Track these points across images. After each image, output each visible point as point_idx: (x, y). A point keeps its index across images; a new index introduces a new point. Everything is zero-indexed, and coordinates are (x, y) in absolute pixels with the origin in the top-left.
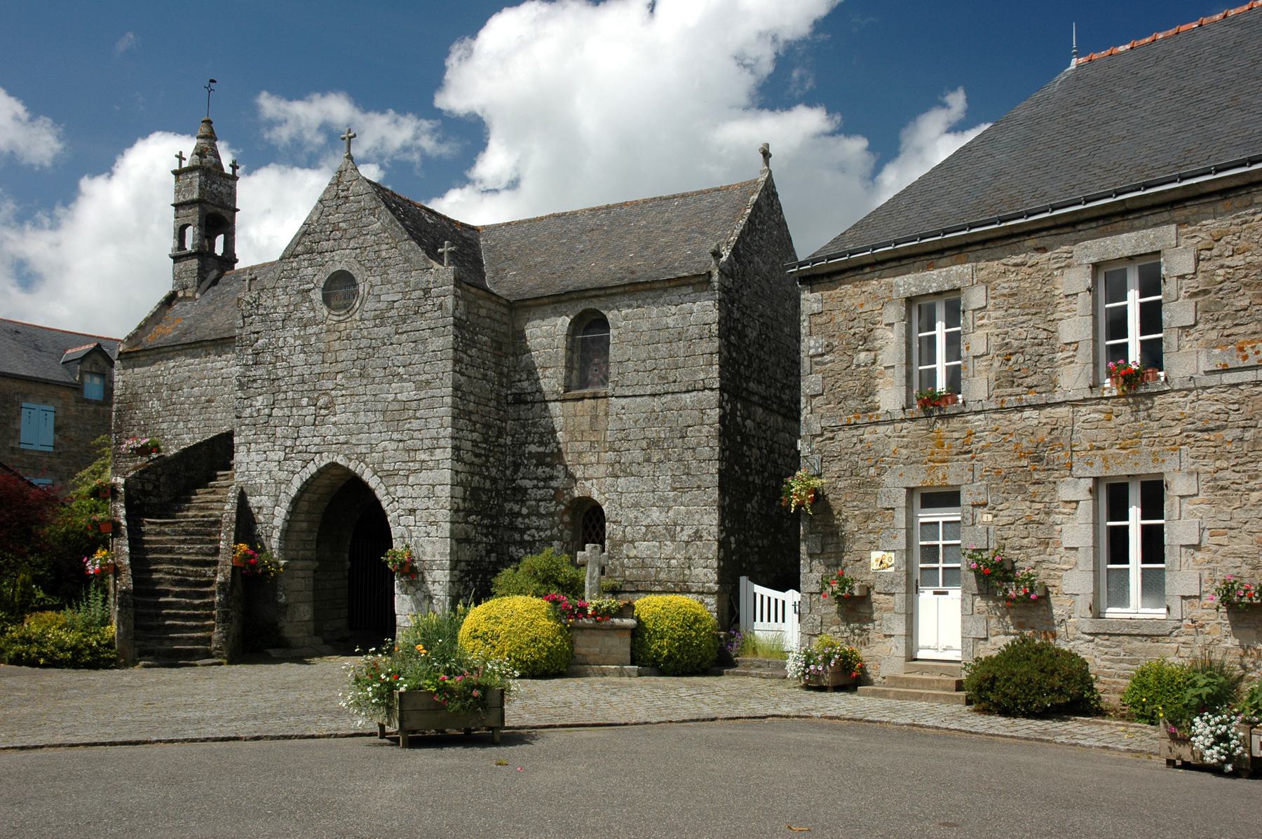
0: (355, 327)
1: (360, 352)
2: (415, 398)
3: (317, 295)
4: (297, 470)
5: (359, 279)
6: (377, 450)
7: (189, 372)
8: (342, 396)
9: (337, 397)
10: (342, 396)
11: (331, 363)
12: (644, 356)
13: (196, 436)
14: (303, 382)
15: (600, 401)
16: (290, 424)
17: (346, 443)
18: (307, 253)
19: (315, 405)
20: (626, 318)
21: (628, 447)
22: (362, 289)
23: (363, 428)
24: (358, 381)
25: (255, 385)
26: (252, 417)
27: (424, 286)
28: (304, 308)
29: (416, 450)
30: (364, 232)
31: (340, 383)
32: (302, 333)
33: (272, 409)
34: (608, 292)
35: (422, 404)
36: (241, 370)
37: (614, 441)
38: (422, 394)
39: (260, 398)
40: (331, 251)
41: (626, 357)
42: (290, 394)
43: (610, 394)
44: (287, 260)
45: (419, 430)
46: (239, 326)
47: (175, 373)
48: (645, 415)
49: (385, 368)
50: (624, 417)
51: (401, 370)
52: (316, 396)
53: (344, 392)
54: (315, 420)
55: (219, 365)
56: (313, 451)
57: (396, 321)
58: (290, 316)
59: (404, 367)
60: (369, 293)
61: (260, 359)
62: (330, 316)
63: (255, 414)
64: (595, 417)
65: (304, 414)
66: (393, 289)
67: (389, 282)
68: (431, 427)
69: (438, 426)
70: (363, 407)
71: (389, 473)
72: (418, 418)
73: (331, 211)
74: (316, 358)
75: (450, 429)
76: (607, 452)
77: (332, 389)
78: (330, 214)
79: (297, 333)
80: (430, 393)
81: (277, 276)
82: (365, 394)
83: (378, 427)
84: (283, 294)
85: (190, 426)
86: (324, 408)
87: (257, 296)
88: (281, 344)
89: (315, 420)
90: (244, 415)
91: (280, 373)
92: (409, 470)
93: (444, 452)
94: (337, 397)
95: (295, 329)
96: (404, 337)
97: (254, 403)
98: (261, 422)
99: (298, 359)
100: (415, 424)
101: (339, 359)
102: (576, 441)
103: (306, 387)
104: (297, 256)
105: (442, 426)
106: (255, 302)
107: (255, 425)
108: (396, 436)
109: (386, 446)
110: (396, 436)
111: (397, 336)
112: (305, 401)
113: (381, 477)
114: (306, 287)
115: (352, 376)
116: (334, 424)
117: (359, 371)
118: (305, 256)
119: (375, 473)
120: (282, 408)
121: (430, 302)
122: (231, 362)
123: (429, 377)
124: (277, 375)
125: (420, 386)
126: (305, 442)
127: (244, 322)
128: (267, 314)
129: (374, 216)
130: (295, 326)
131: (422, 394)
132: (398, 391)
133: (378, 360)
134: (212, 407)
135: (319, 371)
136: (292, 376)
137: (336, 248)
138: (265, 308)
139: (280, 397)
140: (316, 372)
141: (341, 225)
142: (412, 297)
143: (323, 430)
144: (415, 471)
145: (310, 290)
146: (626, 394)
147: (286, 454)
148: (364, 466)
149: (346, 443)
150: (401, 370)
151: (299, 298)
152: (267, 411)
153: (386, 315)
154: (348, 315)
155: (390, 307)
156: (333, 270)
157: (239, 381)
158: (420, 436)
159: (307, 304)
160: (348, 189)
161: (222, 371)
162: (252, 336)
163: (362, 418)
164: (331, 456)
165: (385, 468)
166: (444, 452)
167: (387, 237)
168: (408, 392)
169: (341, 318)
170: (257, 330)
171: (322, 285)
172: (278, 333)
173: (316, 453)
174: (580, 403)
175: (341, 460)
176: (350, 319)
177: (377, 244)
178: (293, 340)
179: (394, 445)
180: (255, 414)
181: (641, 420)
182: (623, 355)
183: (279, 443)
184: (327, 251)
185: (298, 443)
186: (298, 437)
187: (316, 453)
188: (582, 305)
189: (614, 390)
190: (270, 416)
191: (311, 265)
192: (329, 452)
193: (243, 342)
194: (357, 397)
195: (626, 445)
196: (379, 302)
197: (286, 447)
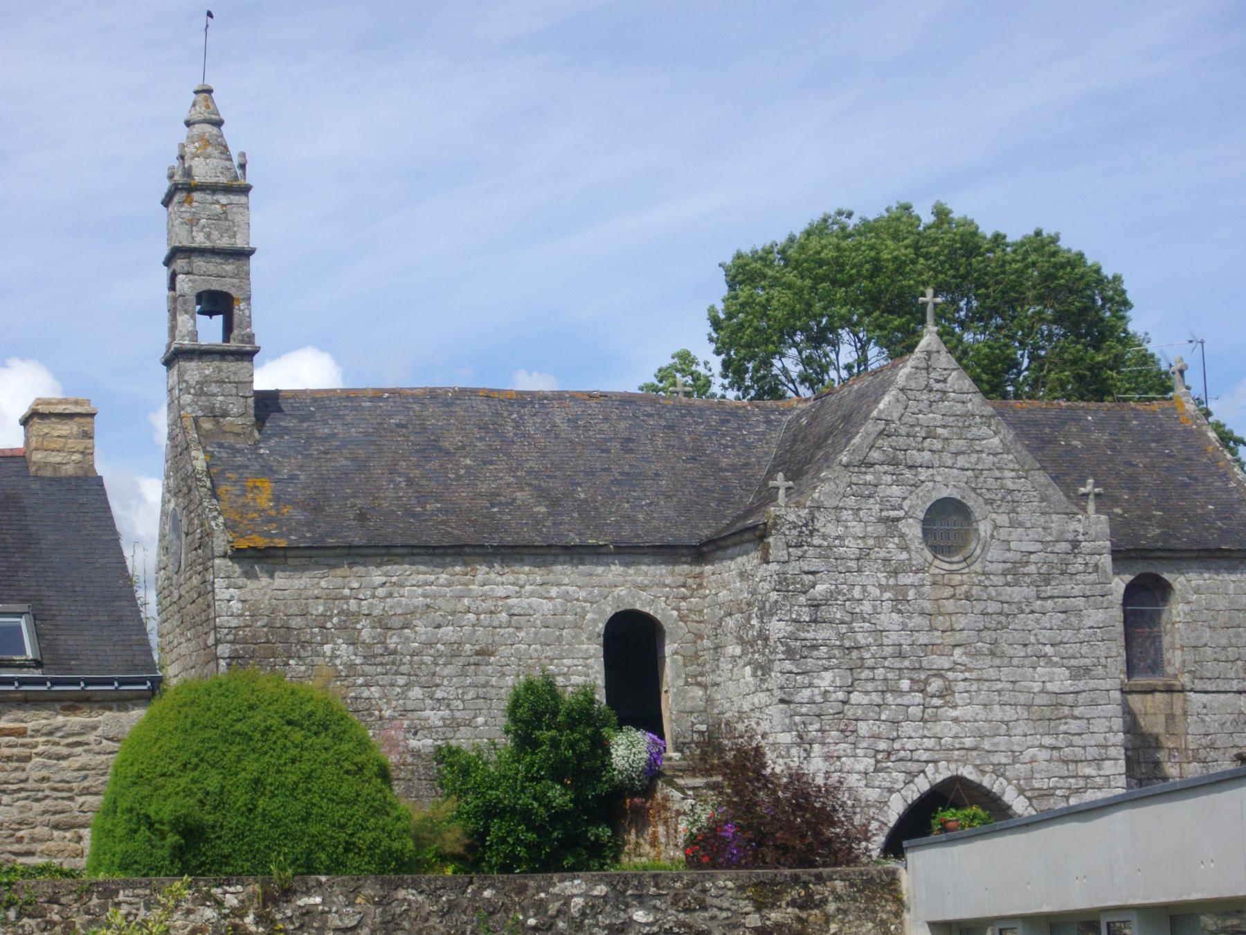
0: (977, 582)
1: (987, 619)
2: (1072, 689)
3: (913, 530)
4: (897, 786)
5: (977, 514)
6: (1022, 761)
7: (425, 596)
8: (965, 680)
9: (956, 681)
10: (965, 680)
11: (943, 632)
12: (1223, 642)
13: (458, 714)
14: (901, 656)
15: (1176, 695)
16: (883, 717)
17: (975, 749)
18: (889, 464)
19: (922, 691)
20: (1197, 591)
21: (1216, 757)
22: (984, 528)
23: (998, 728)
24: (988, 660)
25: (815, 653)
26: (814, 703)
27: (1070, 536)
28: (891, 546)
29: (1076, 762)
30: (978, 448)
31: (959, 661)
32: (892, 581)
33: (849, 693)
34: (1178, 555)
35: (1082, 698)
36: (789, 629)
37: (1198, 749)
38: (1081, 685)
39: (828, 675)
40: (928, 467)
41: (1203, 641)
42: (880, 672)
43: (1188, 688)
44: (856, 469)
45: (1080, 734)
46: (782, 559)
47: (390, 595)
48: (1232, 717)
49: (1025, 645)
50: (1207, 719)
51: (1049, 650)
52: (923, 677)
53: (967, 675)
54: (923, 712)
55: (501, 591)
56: (924, 758)
57: (1035, 581)
58: (868, 554)
59: (1052, 645)
60: (992, 536)
61: (823, 613)
62: (937, 562)
63: (818, 699)
64: (1170, 718)
65: (906, 702)
66: (1028, 535)
67: (1021, 525)
68: (1096, 730)
69: (1106, 730)
70: (997, 698)
71: (1042, 792)
72: (1076, 718)
73: (921, 406)
74: (917, 620)
75: (1121, 735)
76: (1189, 762)
77: (949, 670)
78: (921, 412)
79: (883, 582)
80: (1092, 684)
81: (841, 489)
82: (999, 680)
83: (1021, 728)
84: (854, 520)
85: (439, 694)
86: (938, 697)
87: (809, 517)
88: (857, 593)
89: (923, 712)
90: (798, 698)
91: (862, 639)
92: (1069, 789)
93: (1116, 765)
94: (956, 681)
95: (879, 575)
96: (1050, 603)
97: (816, 681)
98: (831, 711)
99: (891, 620)
100: (1074, 726)
101: (956, 626)
102: (1150, 747)
103: (906, 663)
104: (872, 465)
105: (1111, 730)
106: (806, 525)
107: (818, 716)
108: (1047, 741)
109: (1035, 755)
110: (1047, 741)
111: (1039, 602)
112: (905, 684)
113: (1029, 799)
114: (893, 514)
115: (978, 654)
116: (955, 720)
117: (988, 646)
118: (885, 467)
119: (1021, 792)
120: (867, 693)
121: (1080, 560)
122: (528, 588)
123: (1088, 662)
124: (855, 640)
125: (1079, 673)
126: (910, 745)
127: (789, 554)
128: (829, 547)
129: (989, 427)
130: (878, 569)
131: (1081, 685)
132: (1046, 679)
133: (1015, 633)
134: (488, 664)
135: (926, 641)
136: (881, 645)
137: (936, 464)
138: (824, 537)
139: (863, 676)
140: (921, 641)
141: (939, 431)
142: (1056, 550)
143: (937, 728)
144: (1077, 791)
145: (898, 519)
146: (1209, 689)
147: (877, 762)
148: (1005, 783)
149: (975, 749)
150: (1049, 650)
151: (881, 529)
152: (841, 695)
153: (1021, 570)
154: (964, 564)
155: (1025, 559)
156: (936, 496)
157: (787, 645)
158: (1081, 743)
159: (896, 540)
160: (945, 381)
161: (509, 601)
162: (804, 577)
163: (997, 713)
164: (953, 766)
165: (1036, 784)
166: (1116, 765)
167: (1011, 461)
168: (1060, 680)
169: (955, 567)
170: (814, 569)
171: (921, 516)
172: (851, 578)
173: (927, 762)
174: (1149, 697)
175: (968, 773)
176: (966, 570)
177: (998, 469)
178: (878, 591)
179: (1044, 755)
180: (818, 699)
181: (1228, 724)
182: (1198, 638)
183: (864, 745)
184: (921, 466)
185: (897, 745)
186: (899, 737)
187: (927, 762)
188: (1139, 566)
189: (1193, 683)
190: (844, 703)
191: (896, 483)
192: (948, 761)
193: (788, 585)
194: (987, 684)
195: (1213, 754)
196: (1009, 550)
197: (878, 751)
